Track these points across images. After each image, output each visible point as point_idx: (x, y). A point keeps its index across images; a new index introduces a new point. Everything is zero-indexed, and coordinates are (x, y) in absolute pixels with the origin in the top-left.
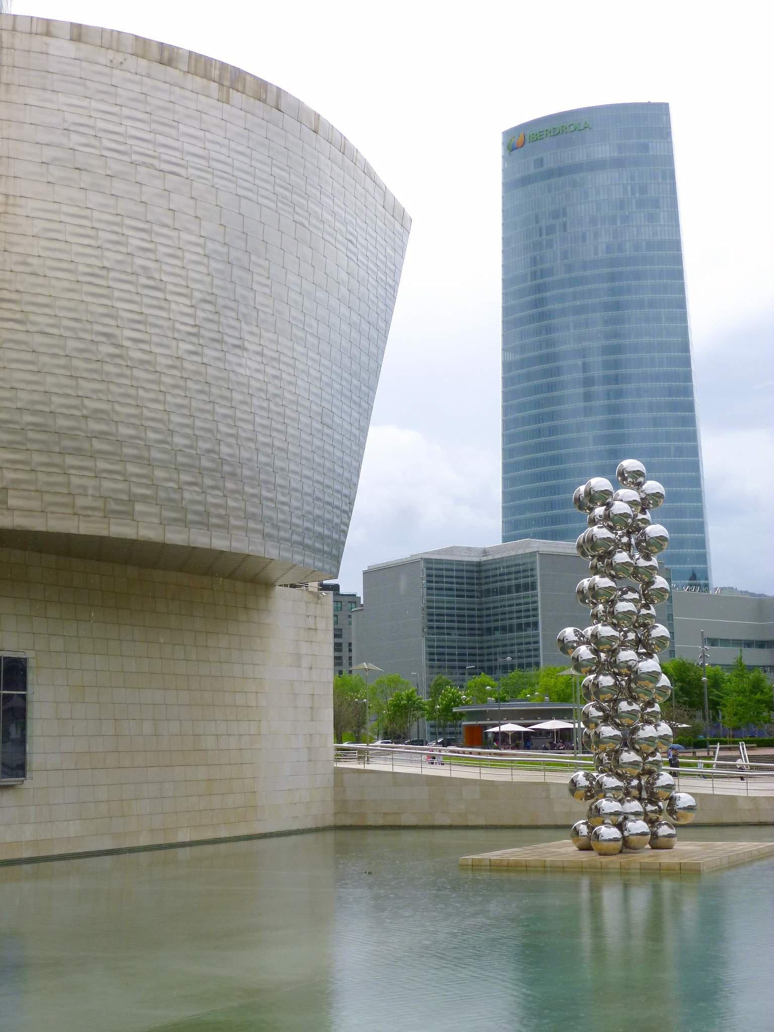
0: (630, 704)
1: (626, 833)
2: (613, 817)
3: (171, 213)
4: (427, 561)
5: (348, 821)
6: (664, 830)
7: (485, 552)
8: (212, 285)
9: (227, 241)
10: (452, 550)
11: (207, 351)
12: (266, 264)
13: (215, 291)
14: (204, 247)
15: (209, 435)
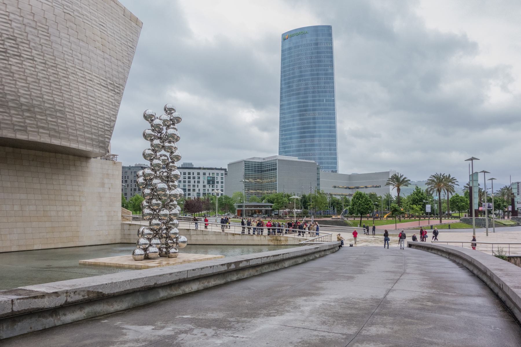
0: (157, 201)
1: (148, 252)
2: (144, 245)
3: (5, 5)
4: (245, 161)
5: (125, 241)
6: (172, 250)
7: (264, 159)
8: (13, 32)
9: (22, 15)
10: (254, 158)
11: (11, 59)
12: (47, 27)
13: (15, 35)
14: (8, 16)
15: (14, 93)
